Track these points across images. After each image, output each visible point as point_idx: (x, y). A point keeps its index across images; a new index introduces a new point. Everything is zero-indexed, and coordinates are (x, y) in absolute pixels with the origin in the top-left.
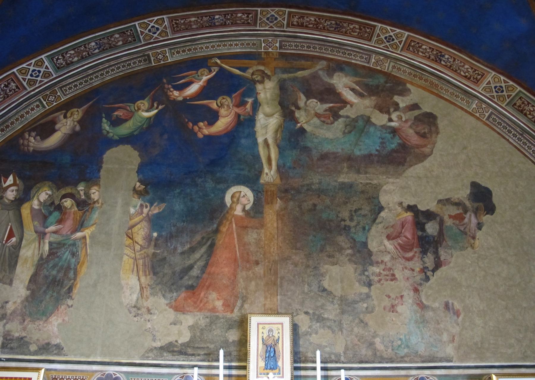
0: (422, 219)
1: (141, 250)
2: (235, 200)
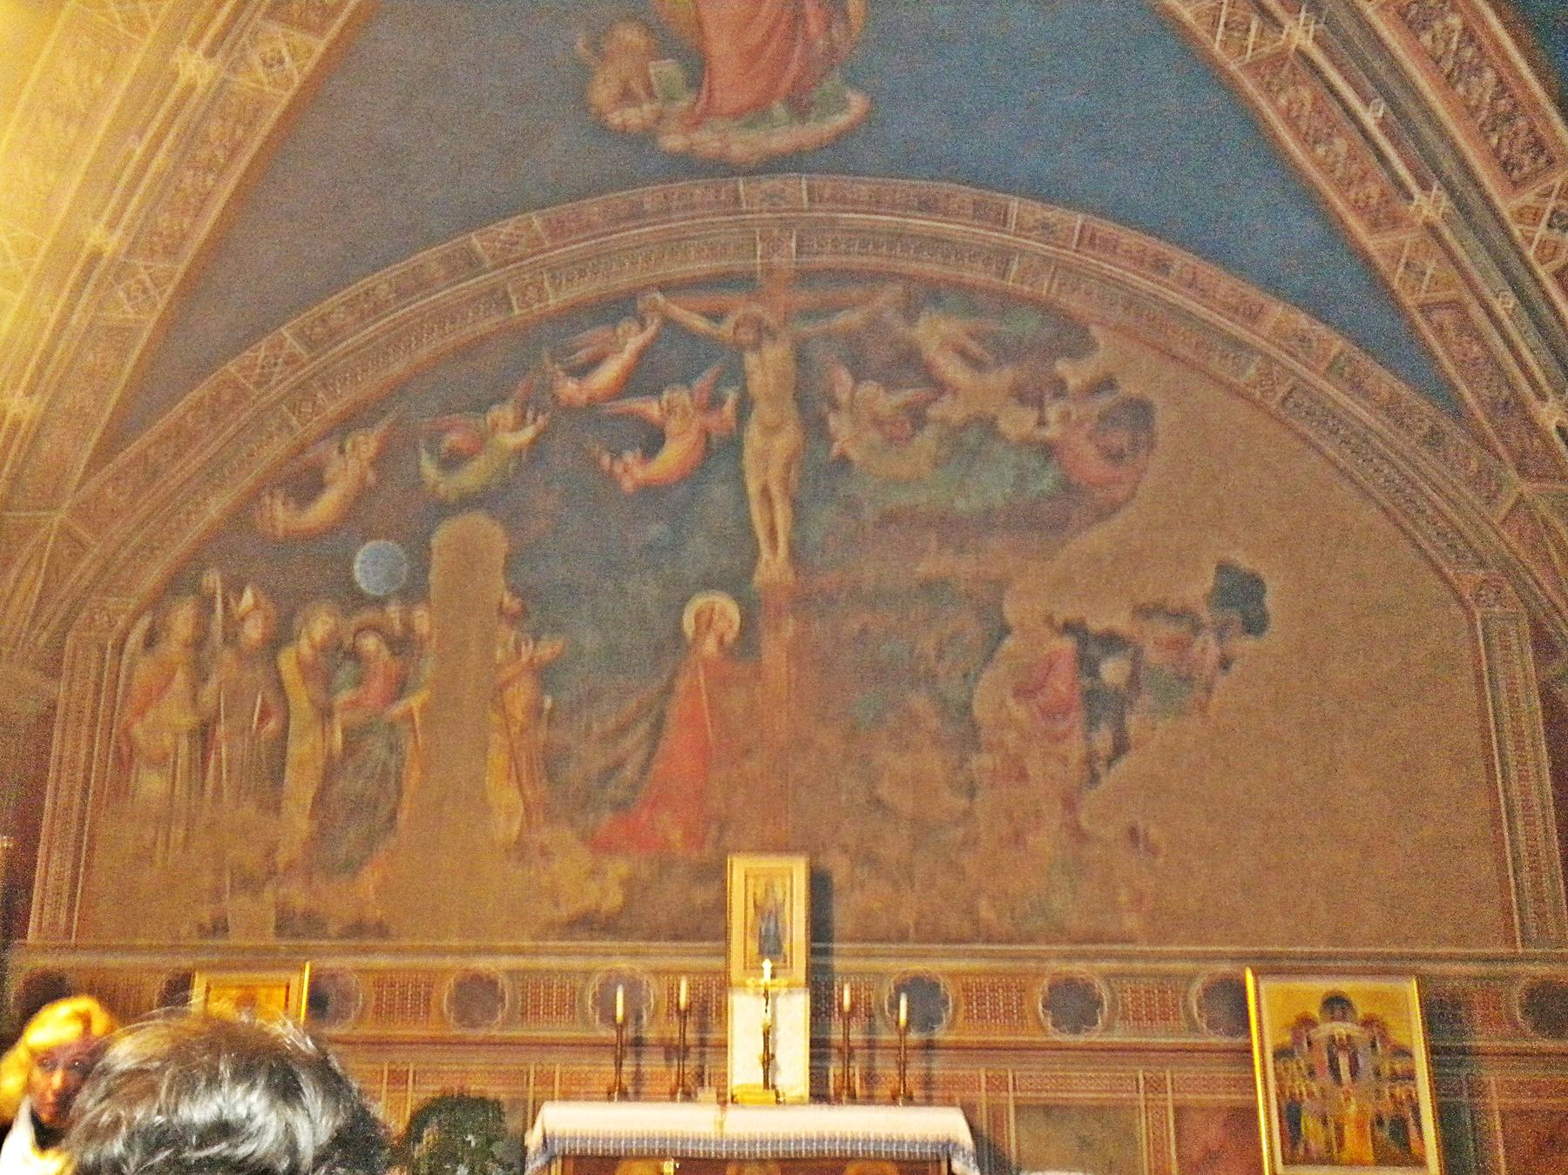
0: (1094, 651)
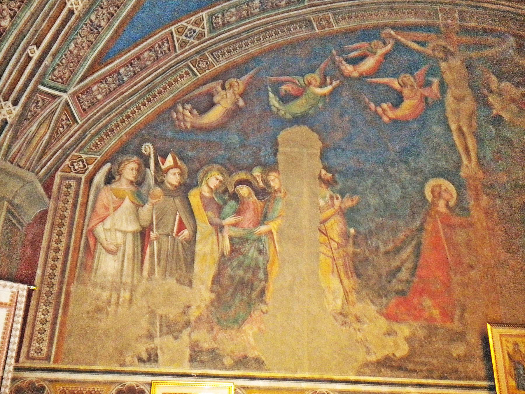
1: (338, 248)
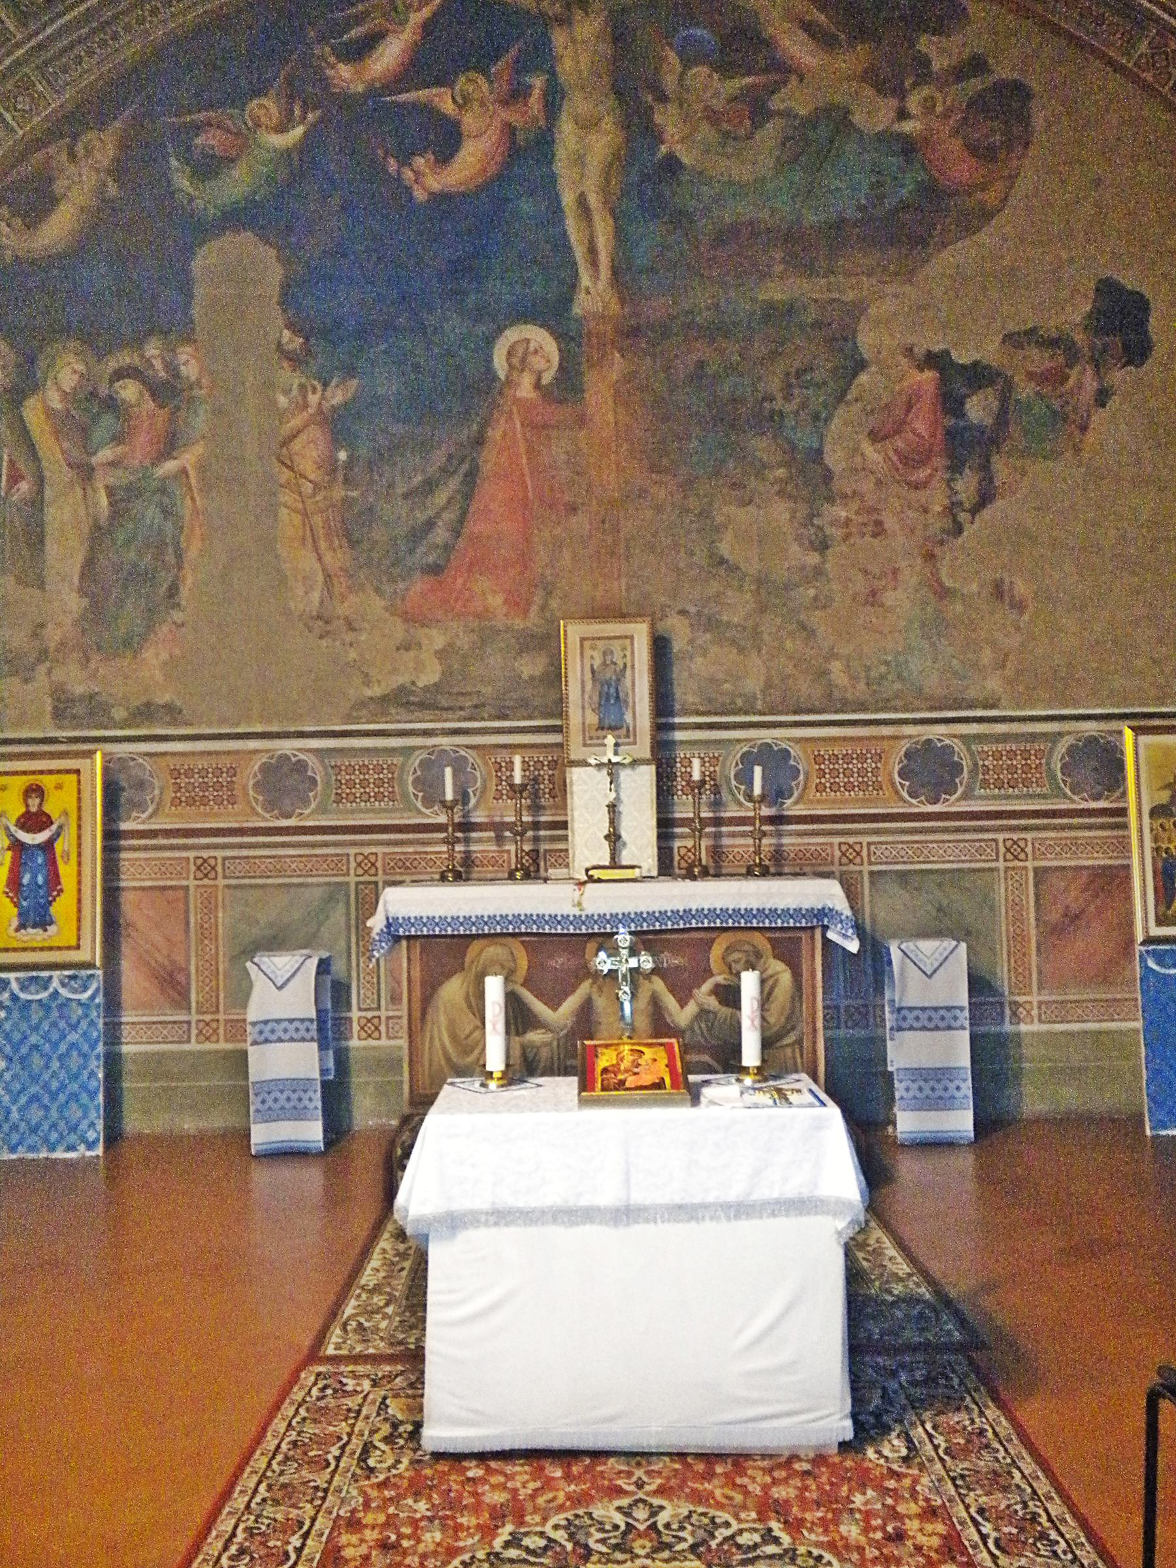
2: (515, 361)
